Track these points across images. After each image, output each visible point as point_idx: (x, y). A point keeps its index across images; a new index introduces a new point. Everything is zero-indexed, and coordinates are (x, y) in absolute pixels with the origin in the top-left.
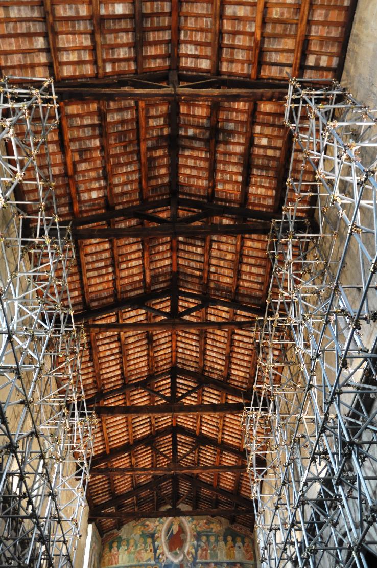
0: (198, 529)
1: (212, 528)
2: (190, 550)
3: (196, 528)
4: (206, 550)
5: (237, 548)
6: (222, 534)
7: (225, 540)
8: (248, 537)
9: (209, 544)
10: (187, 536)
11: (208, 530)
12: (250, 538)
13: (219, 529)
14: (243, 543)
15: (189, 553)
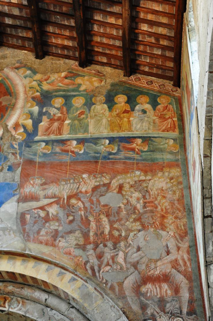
0: (46, 87)
1: (80, 85)
2: (21, 122)
3: (39, 85)
4: (61, 120)
5: (137, 113)
6: (105, 92)
7: (110, 101)
8: (167, 94)
9: (68, 111)
10: (16, 99)
11: (71, 87)
12: (174, 96)
13: (96, 84)
14: (154, 104)
15: (16, 126)
